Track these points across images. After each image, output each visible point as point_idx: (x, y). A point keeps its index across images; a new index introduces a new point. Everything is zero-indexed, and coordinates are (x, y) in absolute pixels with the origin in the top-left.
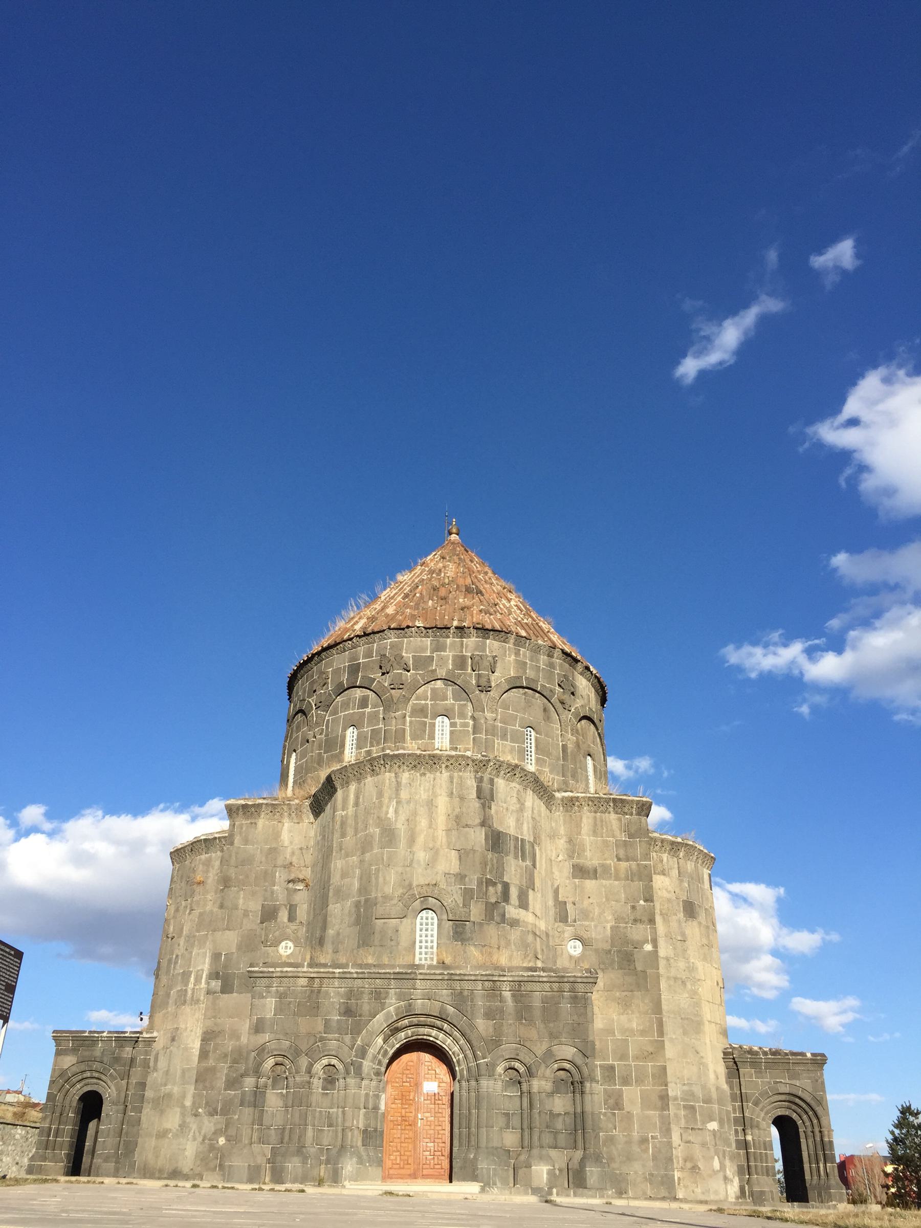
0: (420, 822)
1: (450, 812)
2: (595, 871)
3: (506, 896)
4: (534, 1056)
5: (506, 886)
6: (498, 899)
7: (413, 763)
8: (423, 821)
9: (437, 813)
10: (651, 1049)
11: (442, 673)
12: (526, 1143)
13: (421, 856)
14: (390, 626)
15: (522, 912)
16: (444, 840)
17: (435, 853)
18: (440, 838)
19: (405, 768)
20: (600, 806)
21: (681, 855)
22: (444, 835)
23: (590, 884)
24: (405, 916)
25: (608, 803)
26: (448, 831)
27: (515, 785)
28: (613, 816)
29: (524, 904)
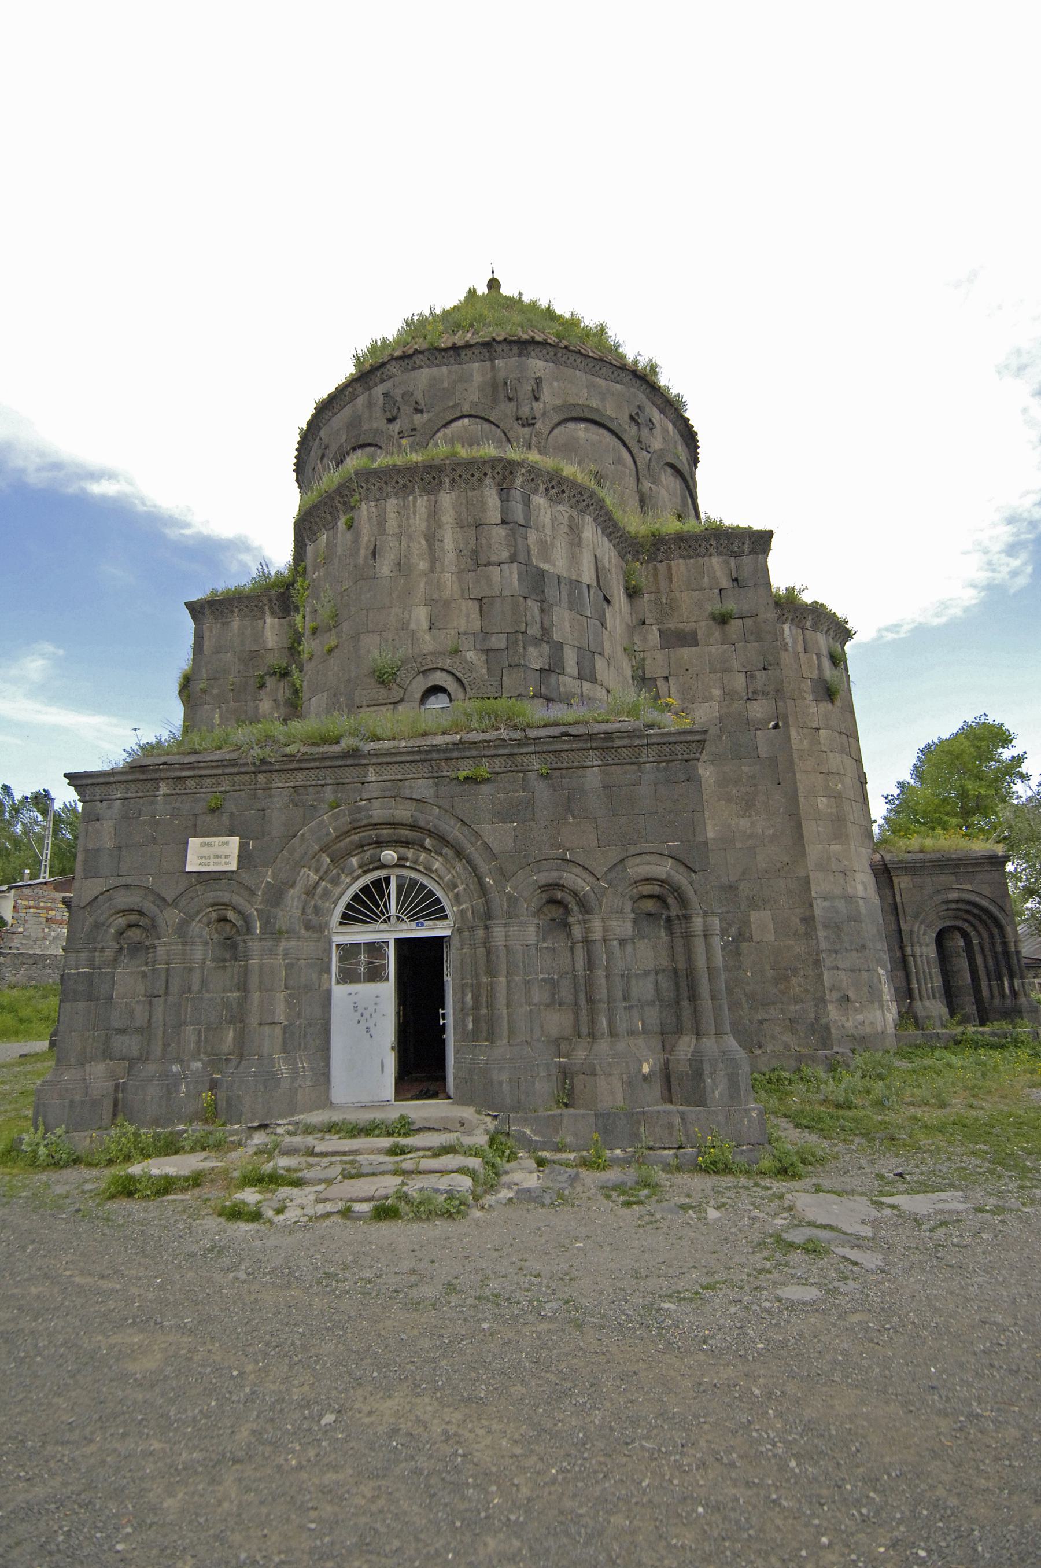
0: (418, 565)
2: (694, 634)
4: (591, 879)
7: (401, 482)
9: (442, 550)
10: (786, 859)
11: (466, 409)
12: (584, 1030)
13: (421, 615)
14: (392, 355)
15: (586, 685)
16: (456, 587)
18: (449, 584)
19: (390, 489)
21: (808, 624)
22: (454, 579)
23: (686, 653)
24: (401, 700)
25: (707, 541)
26: (460, 572)
27: (564, 510)
28: (715, 561)
29: (586, 674)
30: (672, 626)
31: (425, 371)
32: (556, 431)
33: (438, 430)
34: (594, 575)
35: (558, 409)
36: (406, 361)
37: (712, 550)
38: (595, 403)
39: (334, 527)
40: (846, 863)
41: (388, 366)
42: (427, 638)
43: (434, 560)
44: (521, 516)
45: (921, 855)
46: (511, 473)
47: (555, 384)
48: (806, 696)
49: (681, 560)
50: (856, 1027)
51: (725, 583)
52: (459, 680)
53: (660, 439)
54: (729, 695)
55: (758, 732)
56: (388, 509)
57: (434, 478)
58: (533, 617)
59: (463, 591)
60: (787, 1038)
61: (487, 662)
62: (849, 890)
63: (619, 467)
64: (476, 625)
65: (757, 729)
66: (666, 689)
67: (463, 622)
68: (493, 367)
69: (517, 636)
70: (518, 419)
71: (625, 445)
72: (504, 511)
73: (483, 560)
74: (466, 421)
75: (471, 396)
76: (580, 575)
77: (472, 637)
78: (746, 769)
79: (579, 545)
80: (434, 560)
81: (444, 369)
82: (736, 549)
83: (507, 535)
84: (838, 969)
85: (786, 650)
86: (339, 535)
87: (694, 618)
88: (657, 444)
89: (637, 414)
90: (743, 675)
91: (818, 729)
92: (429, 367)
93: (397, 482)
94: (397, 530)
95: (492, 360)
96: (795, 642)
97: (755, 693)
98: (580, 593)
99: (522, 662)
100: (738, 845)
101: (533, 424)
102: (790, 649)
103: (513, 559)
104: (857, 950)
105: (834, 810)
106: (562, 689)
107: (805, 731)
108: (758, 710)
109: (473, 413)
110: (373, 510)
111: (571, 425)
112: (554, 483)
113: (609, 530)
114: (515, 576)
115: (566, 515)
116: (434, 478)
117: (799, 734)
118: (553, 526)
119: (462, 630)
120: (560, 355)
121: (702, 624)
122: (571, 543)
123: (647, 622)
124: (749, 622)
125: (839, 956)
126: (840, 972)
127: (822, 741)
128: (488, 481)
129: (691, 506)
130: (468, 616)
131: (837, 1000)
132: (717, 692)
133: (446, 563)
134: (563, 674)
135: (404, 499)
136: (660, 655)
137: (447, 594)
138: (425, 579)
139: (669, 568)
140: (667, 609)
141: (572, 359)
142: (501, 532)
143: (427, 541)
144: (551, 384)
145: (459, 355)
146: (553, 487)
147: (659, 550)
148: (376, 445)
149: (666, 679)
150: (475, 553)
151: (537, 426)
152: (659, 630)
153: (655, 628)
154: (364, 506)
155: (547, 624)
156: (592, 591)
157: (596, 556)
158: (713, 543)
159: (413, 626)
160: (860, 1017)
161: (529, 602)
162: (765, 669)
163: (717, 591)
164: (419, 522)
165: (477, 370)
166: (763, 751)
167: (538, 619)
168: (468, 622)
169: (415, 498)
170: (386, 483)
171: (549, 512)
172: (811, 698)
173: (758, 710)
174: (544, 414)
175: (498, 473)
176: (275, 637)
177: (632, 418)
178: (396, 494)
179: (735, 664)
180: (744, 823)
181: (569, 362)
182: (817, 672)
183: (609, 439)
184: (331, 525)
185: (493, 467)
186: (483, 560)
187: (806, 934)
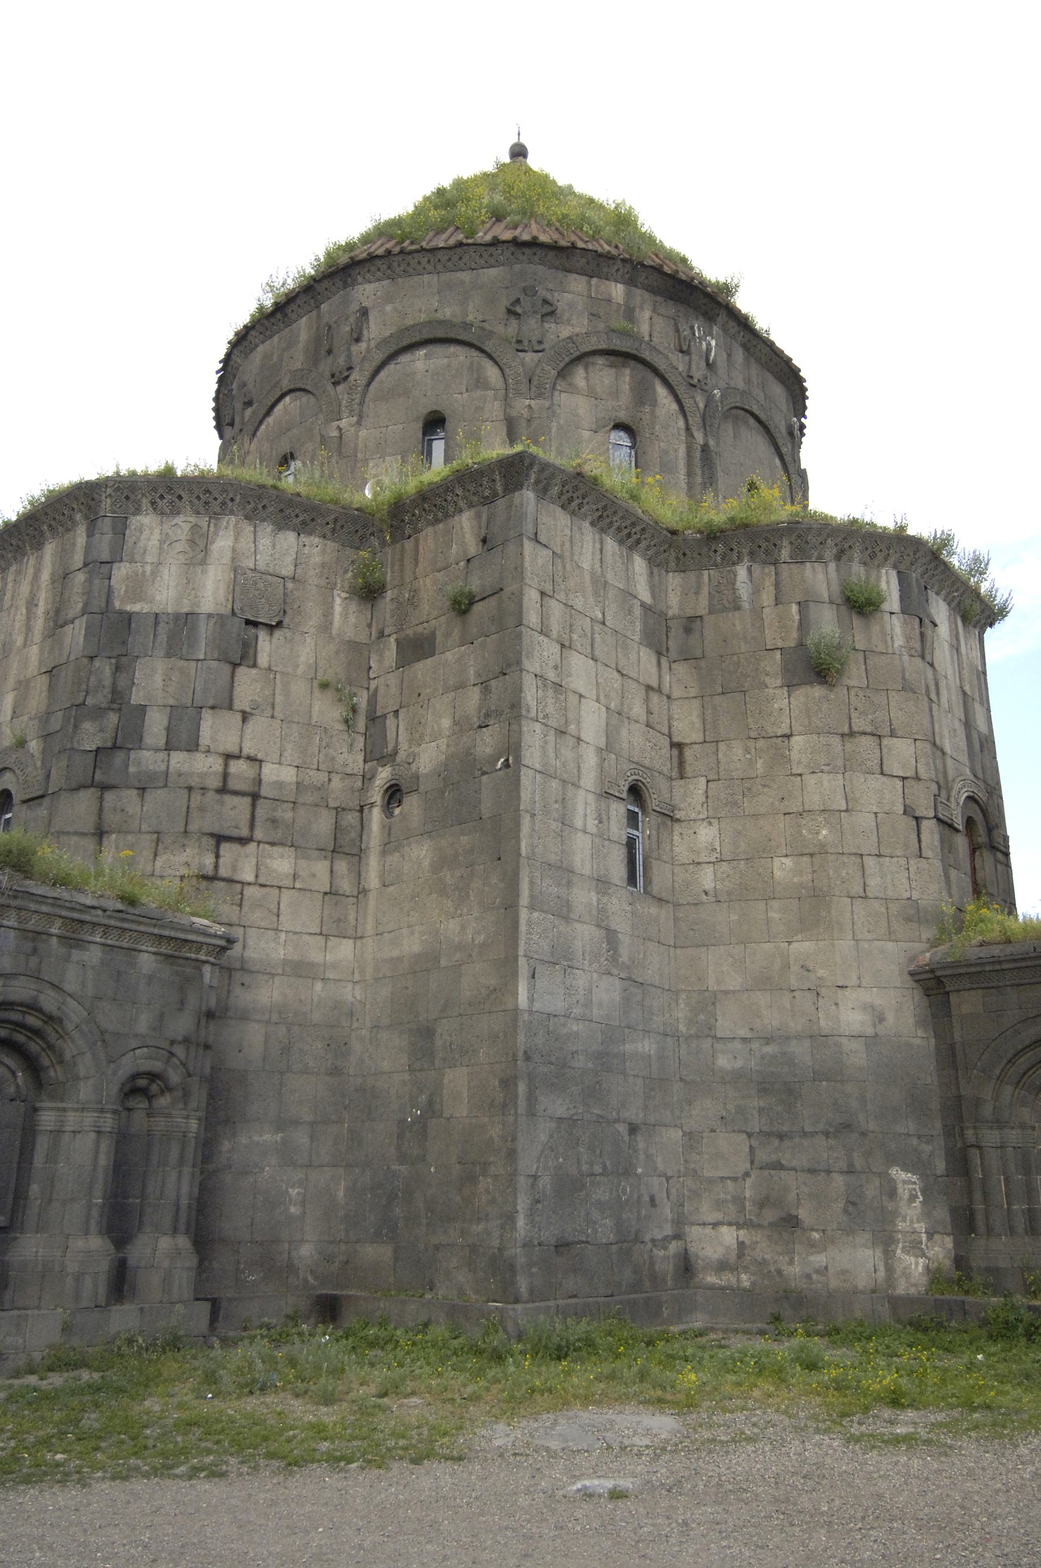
10: (493, 982)
11: (286, 384)
21: (785, 554)
23: (422, 669)
30: (410, 632)
31: (261, 348)
32: (382, 374)
33: (261, 423)
35: (385, 341)
36: (244, 344)
37: (462, 504)
38: (448, 313)
40: (821, 973)
43: (29, 629)
45: (1009, 949)
47: (389, 308)
48: (767, 680)
50: (808, 1277)
51: (473, 548)
55: (485, 778)
60: (462, 1277)
62: (822, 1023)
63: (478, 393)
65: (484, 773)
68: (319, 316)
69: (78, 712)
71: (490, 357)
72: (88, 548)
73: (61, 622)
74: (287, 399)
75: (298, 360)
78: (464, 839)
79: (203, 562)
80: (29, 629)
81: (276, 338)
84: (778, 1166)
85: (738, 608)
90: (477, 689)
91: (788, 736)
92: (263, 342)
95: (318, 307)
96: (756, 591)
97: (487, 715)
98: (194, 629)
100: (444, 963)
101: (348, 377)
102: (746, 605)
104: (827, 1135)
105: (807, 878)
106: (132, 769)
107: (761, 743)
111: (404, 358)
112: (161, 491)
114: (83, 632)
117: (747, 751)
118: (161, 548)
120: (395, 264)
121: (443, 619)
122: (190, 564)
123: (386, 633)
125: (787, 1143)
126: (783, 1174)
127: (795, 755)
131: (772, 1225)
132: (446, 723)
134: (140, 749)
136: (393, 679)
141: (414, 263)
145: (286, 315)
149: (396, 712)
150: (57, 612)
151: (352, 378)
152: (397, 641)
153: (392, 639)
155: (122, 683)
158: (459, 492)
160: (819, 1259)
161: (97, 663)
164: (25, 589)
165: (303, 328)
166: (486, 807)
167: (108, 682)
171: (157, 531)
172: (779, 682)
178: (15, 559)
180: (453, 926)
181: (409, 269)
182: (795, 635)
187: (504, 1106)
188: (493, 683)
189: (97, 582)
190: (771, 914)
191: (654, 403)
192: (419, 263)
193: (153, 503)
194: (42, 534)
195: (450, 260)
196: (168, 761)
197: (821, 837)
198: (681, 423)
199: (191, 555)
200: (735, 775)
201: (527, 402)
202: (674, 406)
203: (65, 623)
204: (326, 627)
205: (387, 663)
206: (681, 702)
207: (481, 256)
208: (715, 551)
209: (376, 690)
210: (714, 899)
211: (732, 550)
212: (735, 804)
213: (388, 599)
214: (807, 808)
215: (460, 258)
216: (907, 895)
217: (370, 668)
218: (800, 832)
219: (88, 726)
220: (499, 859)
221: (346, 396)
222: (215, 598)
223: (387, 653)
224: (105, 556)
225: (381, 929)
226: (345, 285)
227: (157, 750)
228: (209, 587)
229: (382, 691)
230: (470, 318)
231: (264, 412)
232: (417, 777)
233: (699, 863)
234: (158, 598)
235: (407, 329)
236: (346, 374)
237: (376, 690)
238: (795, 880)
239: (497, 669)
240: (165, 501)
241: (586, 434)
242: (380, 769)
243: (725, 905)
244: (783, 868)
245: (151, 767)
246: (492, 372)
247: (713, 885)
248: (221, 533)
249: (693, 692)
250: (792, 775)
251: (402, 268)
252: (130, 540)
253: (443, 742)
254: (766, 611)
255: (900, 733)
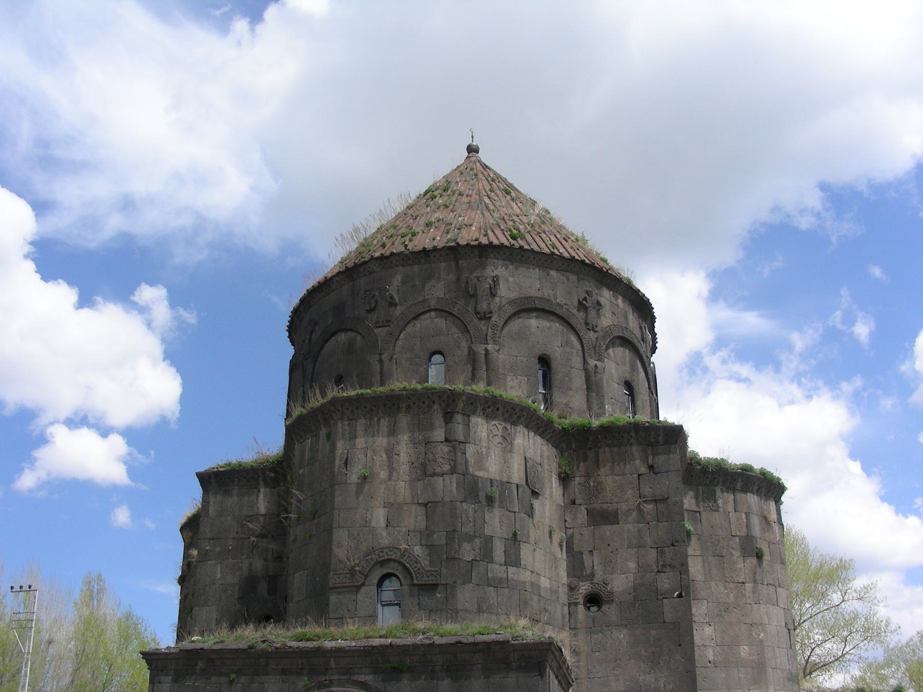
1: (413, 459)
3: (487, 554)
5: (489, 540)
6: (476, 557)
8: (382, 473)
11: (433, 303)
14: (372, 256)
15: (511, 570)
17: (394, 509)
19: (360, 412)
20: (620, 437)
22: (407, 487)
23: (608, 529)
24: (363, 584)
29: (513, 560)
30: (597, 505)
34: (523, 475)
35: (512, 302)
37: (632, 441)
39: (317, 436)
41: (369, 264)
42: (384, 534)
43: (391, 469)
44: (461, 434)
46: (454, 401)
47: (511, 279)
49: (607, 449)
52: (406, 569)
53: (609, 315)
54: (642, 567)
55: (665, 600)
56: (358, 428)
57: (394, 404)
58: (468, 518)
59: (413, 498)
61: (429, 555)
63: (568, 349)
64: (423, 525)
65: (664, 598)
66: (590, 562)
67: (412, 521)
70: (477, 313)
73: (430, 471)
76: (510, 477)
77: (418, 533)
78: (653, 632)
79: (511, 451)
80: (391, 469)
81: (416, 268)
82: (652, 440)
83: (450, 451)
86: (320, 443)
87: (616, 500)
88: (606, 321)
89: (585, 299)
90: (654, 551)
93: (365, 407)
94: (365, 446)
97: (663, 566)
98: (510, 492)
99: (457, 556)
101: (490, 318)
103: (453, 471)
106: (490, 575)
107: (732, 585)
108: (665, 582)
109: (439, 307)
110: (347, 428)
112: (490, 403)
113: (541, 430)
114: (454, 485)
115: (500, 427)
116: (394, 404)
119: (411, 528)
122: (504, 451)
123: (577, 502)
124: (661, 506)
128: (436, 407)
129: (641, 370)
130: (416, 517)
132: (632, 565)
133: (401, 472)
135: (370, 419)
137: (400, 499)
138: (384, 486)
139: (597, 454)
140: (594, 492)
142: (445, 449)
143: (387, 454)
144: (507, 280)
145: (428, 257)
146: (489, 407)
147: (588, 439)
148: (356, 331)
150: (424, 465)
151: (493, 319)
152: (587, 509)
154: (340, 424)
156: (520, 490)
157: (525, 459)
158: (633, 434)
159: (374, 524)
162: (673, 545)
163: (635, 476)
166: (668, 616)
168: (416, 522)
169: (379, 420)
170: (357, 408)
171: (485, 427)
172: (739, 554)
173: (665, 582)
174: (500, 308)
175: (444, 401)
176: (266, 504)
177: (580, 302)
179: (648, 540)
182: (745, 530)
183: (557, 326)
184: (314, 433)
185: (440, 397)
186: (430, 471)
188: (666, 549)
189: (459, 454)
190: (740, 675)
191: (638, 372)
192: (529, 257)
193: (483, 409)
194: (399, 408)
195: (546, 261)
196: (507, 572)
197: (761, 637)
198: (647, 386)
199: (504, 445)
200: (721, 600)
201: (595, 362)
202: (644, 374)
203: (434, 474)
204: (551, 496)
205: (579, 521)
206: (693, 557)
207: (563, 264)
208: (707, 477)
209: (572, 536)
210: (713, 665)
211: (715, 478)
212: (721, 616)
213: (576, 483)
214: (754, 622)
215: (552, 262)
216: (788, 668)
217: (566, 521)
218: (751, 634)
219: (466, 546)
220: (680, 645)
221: (490, 330)
222: (519, 475)
223: (579, 516)
224: (462, 439)
225: (591, 675)
226: (481, 257)
227: (501, 565)
228: (515, 468)
229: (577, 537)
230: (558, 300)
231: (412, 317)
232: (611, 593)
233: (706, 646)
234: (491, 470)
235: (527, 298)
236: (490, 315)
237: (572, 536)
238: (751, 658)
239: (669, 543)
240: (490, 409)
241: (616, 385)
242: (581, 584)
243: (719, 669)
244: (744, 651)
245: (499, 575)
246: (573, 339)
247: (713, 658)
248: (518, 435)
249: (698, 553)
250: (746, 603)
251: (519, 257)
252: (472, 431)
253: (631, 577)
254: (731, 514)
255: (782, 586)
